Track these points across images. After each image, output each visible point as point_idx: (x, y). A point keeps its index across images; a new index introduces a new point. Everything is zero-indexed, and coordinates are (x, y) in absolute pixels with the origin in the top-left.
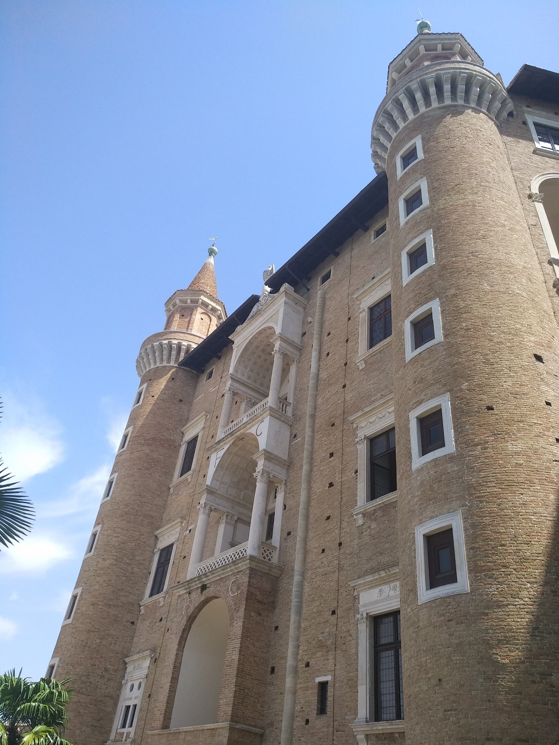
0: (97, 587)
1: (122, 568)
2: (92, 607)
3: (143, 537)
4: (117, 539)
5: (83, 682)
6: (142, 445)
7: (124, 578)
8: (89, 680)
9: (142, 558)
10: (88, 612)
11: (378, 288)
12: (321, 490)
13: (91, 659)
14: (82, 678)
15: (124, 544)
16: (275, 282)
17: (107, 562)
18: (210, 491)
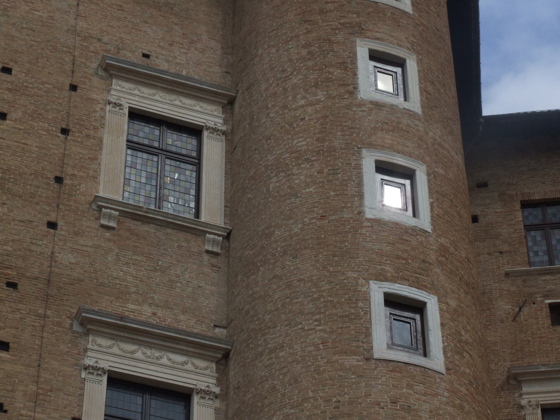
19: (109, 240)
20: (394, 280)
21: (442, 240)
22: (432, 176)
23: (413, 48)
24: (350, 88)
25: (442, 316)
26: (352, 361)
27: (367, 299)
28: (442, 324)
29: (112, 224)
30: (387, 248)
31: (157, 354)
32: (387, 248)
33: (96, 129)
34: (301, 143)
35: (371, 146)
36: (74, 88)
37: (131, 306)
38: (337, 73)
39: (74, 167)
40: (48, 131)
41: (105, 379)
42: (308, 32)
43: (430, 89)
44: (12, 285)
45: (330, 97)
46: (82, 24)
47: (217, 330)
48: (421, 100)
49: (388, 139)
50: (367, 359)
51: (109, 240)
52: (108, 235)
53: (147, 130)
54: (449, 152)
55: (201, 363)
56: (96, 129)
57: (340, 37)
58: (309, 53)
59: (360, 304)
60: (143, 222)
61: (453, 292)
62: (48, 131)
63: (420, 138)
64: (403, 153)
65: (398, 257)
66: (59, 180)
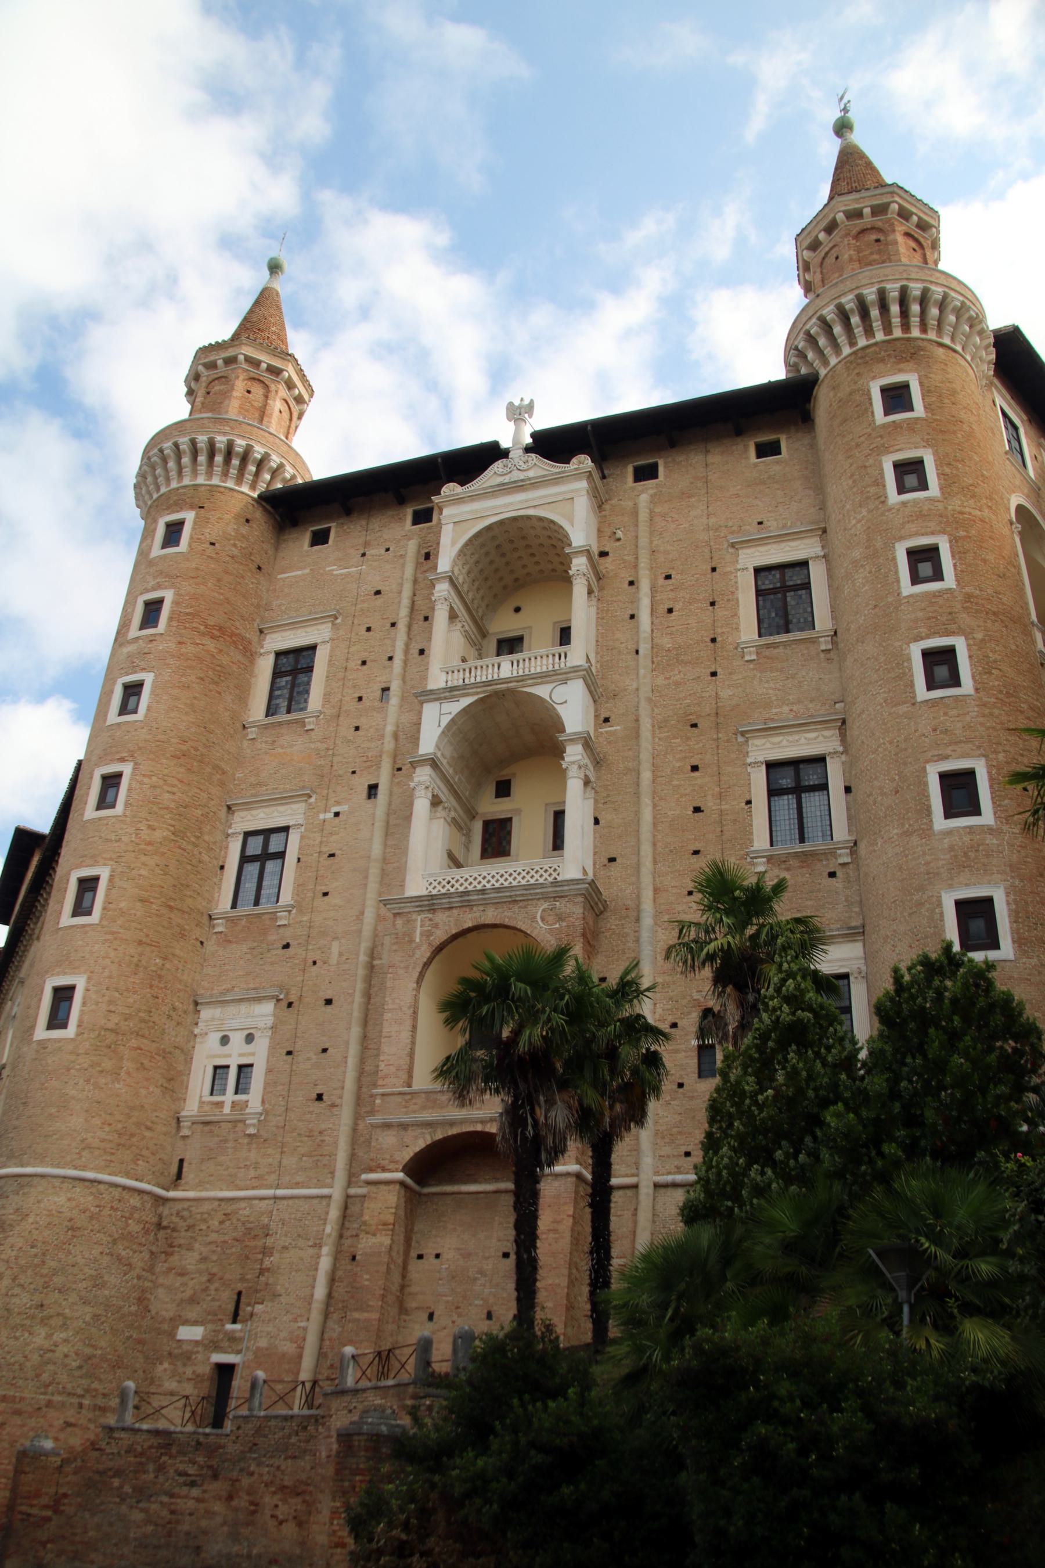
0: (143, 872)
1: (184, 850)
2: (139, 904)
3: (212, 803)
4: (171, 796)
5: (143, 1021)
6: (203, 634)
7: (189, 867)
8: (152, 1019)
9: (212, 839)
10: (133, 912)
11: (774, 546)
12: (678, 812)
13: (151, 986)
14: (142, 1014)
15: (185, 808)
16: (554, 445)
17: (158, 835)
18: (434, 763)
19: (753, 669)
20: (928, 637)
21: (967, 590)
22: (954, 542)
23: (928, 444)
24: (883, 499)
25: (969, 650)
26: (904, 709)
27: (909, 660)
28: (970, 657)
29: (754, 657)
30: (920, 614)
31: (796, 737)
32: (920, 614)
33: (733, 593)
34: (857, 554)
35: (902, 538)
36: (714, 570)
37: (774, 711)
38: (872, 490)
39: (722, 627)
40: (701, 608)
41: (764, 767)
42: (851, 465)
43: (947, 470)
44: (694, 726)
45: (870, 511)
46: (713, 520)
47: (837, 705)
48: (940, 484)
49: (913, 527)
50: (913, 704)
51: (753, 669)
52: (752, 666)
53: (771, 577)
54: (970, 514)
55: (827, 733)
56: (733, 593)
57: (871, 461)
58: (854, 482)
59: (906, 664)
60: (775, 648)
61: (979, 626)
62: (701, 608)
63: (941, 516)
64: (927, 534)
65: (929, 618)
66: (713, 640)
